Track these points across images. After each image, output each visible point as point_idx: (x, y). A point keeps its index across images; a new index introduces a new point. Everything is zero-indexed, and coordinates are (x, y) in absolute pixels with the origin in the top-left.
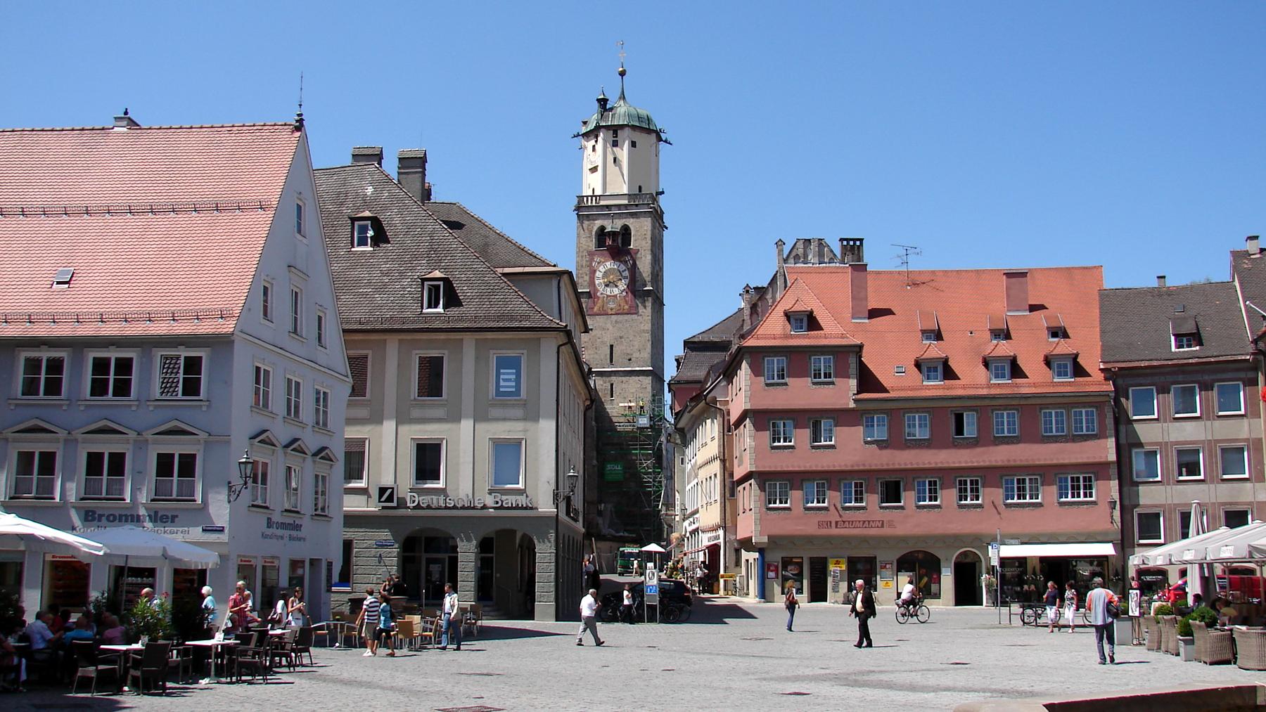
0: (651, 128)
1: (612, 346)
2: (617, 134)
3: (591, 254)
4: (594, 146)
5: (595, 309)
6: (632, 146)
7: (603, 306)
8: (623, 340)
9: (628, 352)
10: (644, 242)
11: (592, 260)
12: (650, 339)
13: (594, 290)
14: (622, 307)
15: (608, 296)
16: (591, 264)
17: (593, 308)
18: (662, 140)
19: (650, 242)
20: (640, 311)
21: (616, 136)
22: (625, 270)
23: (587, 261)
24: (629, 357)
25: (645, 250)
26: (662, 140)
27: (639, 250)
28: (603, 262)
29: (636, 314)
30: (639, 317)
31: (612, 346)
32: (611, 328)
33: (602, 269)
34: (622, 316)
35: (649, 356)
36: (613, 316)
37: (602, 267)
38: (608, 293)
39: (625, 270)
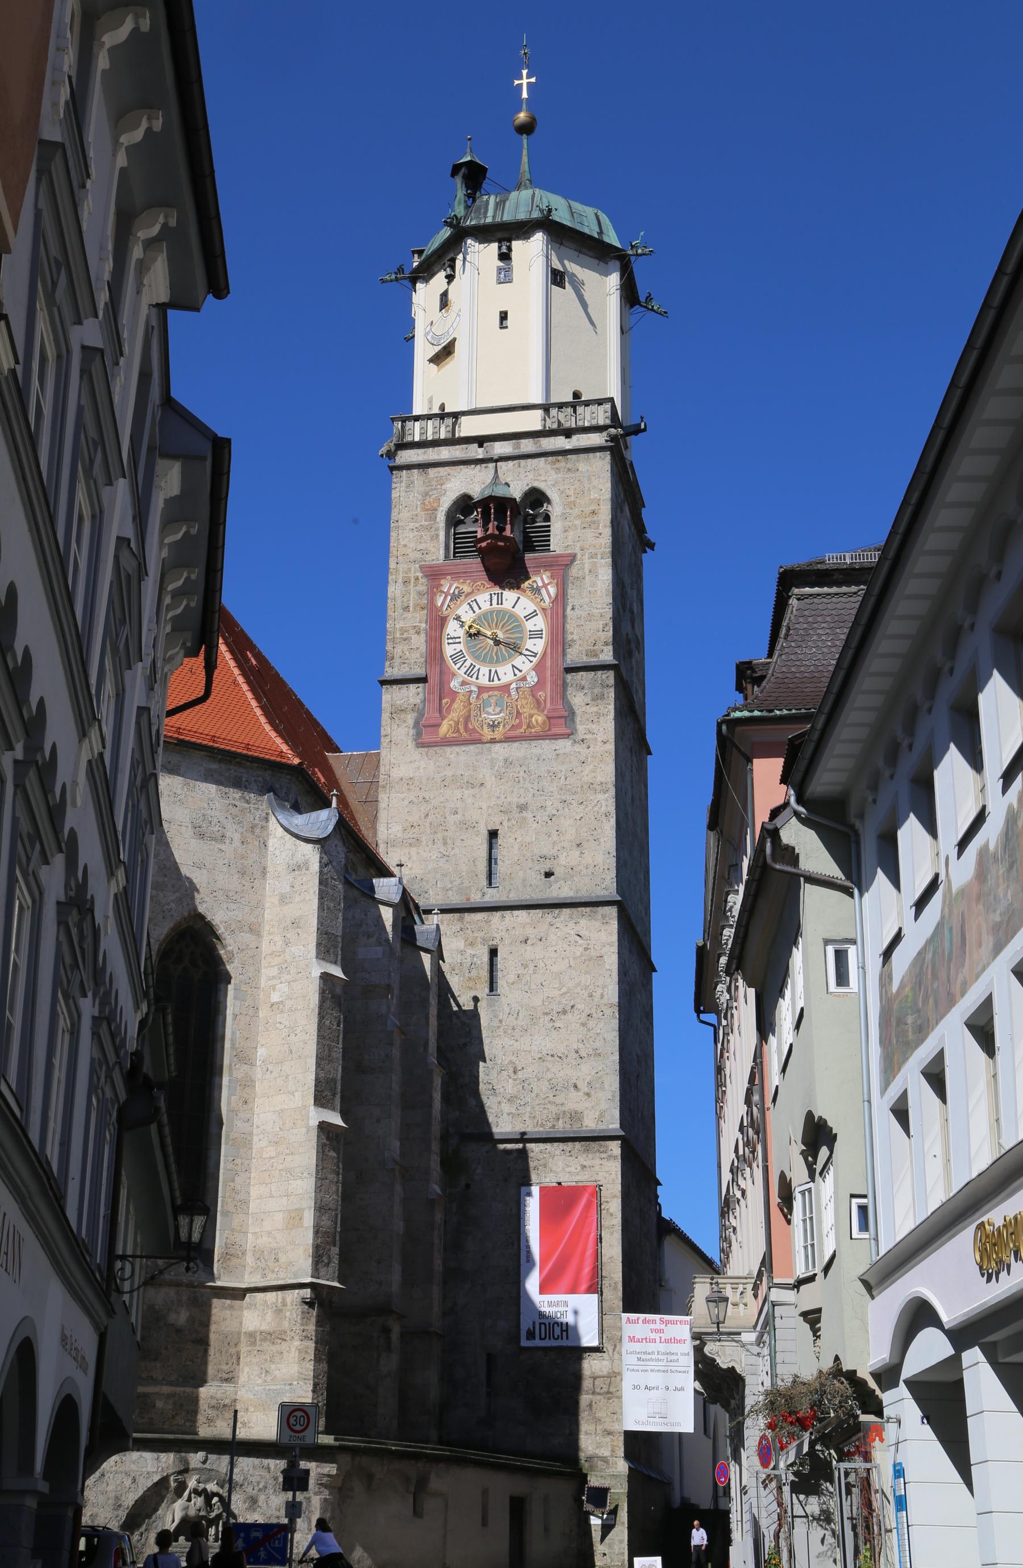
0: (606, 239)
1: (493, 835)
2: (510, 249)
3: (434, 575)
4: (444, 295)
5: (444, 728)
7: (467, 719)
8: (528, 815)
9: (545, 852)
10: (590, 534)
11: (434, 588)
13: (441, 673)
15: (482, 689)
17: (438, 725)
18: (639, 303)
19: (607, 532)
20: (581, 729)
21: (505, 257)
22: (534, 614)
23: (419, 593)
24: (546, 867)
25: (593, 556)
28: (468, 595)
29: (567, 736)
30: (579, 748)
31: (493, 835)
32: (490, 781)
34: (525, 744)
37: (465, 607)
38: (484, 681)
39: (534, 614)
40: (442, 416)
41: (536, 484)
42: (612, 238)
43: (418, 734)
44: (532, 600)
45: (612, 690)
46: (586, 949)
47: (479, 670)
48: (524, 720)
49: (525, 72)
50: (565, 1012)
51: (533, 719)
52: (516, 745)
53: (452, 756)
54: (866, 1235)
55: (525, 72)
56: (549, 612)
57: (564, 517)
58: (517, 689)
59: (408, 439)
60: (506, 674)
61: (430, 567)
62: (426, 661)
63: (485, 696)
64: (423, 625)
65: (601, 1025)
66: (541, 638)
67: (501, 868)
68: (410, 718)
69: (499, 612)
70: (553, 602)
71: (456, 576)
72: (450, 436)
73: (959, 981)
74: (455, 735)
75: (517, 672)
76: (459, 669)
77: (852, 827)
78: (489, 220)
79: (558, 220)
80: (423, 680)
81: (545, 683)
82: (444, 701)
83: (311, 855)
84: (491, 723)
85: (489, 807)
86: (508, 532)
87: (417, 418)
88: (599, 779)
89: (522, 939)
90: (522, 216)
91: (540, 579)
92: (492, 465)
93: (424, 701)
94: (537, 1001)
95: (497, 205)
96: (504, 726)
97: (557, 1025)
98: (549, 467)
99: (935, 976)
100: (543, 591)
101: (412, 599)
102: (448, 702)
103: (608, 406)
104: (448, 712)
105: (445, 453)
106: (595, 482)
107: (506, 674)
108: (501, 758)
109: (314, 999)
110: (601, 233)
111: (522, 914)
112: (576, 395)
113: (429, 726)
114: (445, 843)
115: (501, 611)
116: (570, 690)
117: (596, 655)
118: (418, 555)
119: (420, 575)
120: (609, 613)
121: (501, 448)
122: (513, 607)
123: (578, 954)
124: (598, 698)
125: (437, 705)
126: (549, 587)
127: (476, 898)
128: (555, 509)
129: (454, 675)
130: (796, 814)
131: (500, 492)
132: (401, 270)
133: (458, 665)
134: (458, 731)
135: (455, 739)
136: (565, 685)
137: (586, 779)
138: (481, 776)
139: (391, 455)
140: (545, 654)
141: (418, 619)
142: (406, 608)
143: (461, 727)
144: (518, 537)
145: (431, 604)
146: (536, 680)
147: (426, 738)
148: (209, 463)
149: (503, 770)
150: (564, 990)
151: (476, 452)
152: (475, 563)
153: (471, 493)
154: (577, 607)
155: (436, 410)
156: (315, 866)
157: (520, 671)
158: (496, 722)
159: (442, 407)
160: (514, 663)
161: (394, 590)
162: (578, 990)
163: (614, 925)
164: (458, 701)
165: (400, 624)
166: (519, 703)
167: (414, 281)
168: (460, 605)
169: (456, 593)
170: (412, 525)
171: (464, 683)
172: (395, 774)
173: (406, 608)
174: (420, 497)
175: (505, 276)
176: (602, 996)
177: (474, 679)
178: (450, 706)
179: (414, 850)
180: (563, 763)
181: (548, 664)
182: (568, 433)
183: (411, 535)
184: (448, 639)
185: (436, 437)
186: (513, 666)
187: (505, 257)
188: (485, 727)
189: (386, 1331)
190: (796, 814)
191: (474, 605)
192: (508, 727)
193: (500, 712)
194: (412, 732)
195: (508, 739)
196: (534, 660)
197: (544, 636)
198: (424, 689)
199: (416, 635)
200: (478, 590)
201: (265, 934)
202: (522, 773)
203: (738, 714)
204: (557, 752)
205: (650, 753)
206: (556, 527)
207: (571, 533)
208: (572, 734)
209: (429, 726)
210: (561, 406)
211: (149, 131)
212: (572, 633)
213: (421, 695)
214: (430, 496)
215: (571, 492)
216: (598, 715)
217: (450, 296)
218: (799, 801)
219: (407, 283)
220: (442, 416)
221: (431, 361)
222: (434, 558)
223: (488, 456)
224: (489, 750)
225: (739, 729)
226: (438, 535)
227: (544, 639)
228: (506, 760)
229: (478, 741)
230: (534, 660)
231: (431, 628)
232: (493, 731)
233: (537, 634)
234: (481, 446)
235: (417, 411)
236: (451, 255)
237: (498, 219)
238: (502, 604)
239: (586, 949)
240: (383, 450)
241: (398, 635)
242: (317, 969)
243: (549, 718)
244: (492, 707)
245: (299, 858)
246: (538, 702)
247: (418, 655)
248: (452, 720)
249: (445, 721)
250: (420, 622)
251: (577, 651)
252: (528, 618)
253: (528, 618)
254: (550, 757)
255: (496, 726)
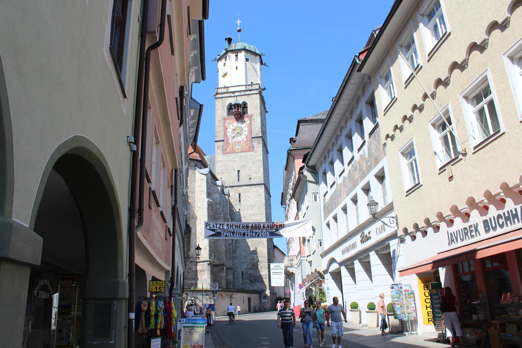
0: (256, 52)
1: (239, 171)
2: (237, 54)
3: (224, 119)
5: (228, 150)
6: (247, 61)
7: (233, 148)
10: (256, 110)
11: (225, 122)
12: (262, 165)
13: (227, 139)
14: (244, 148)
15: (235, 142)
16: (224, 125)
17: (227, 150)
18: (263, 64)
19: (259, 110)
20: (255, 149)
21: (236, 56)
23: (222, 123)
26: (263, 64)
27: (253, 115)
28: (232, 123)
30: (255, 153)
31: (239, 171)
33: (231, 127)
34: (244, 153)
35: (263, 176)
36: (239, 154)
37: (231, 126)
38: (236, 140)
40: (225, 88)
41: (245, 101)
42: (258, 52)
43: (223, 151)
45: (261, 141)
46: (258, 193)
49: (239, 20)
50: (254, 206)
52: (243, 153)
54: (321, 247)
55: (239, 20)
57: (250, 107)
59: (218, 92)
60: (240, 139)
61: (224, 118)
63: (236, 143)
64: (223, 129)
65: (262, 208)
67: (240, 178)
68: (221, 148)
69: (238, 126)
71: (229, 119)
72: (227, 91)
73: (340, 200)
77: (317, 171)
78: (233, 49)
79: (247, 48)
80: (223, 141)
81: (248, 141)
83: (205, 177)
85: (237, 166)
86: (239, 111)
87: (220, 88)
88: (259, 159)
89: (245, 192)
90: (240, 48)
91: (246, 119)
92: (235, 97)
93: (224, 145)
94: (249, 204)
95: (234, 46)
97: (253, 208)
98: (247, 97)
99: (335, 200)
100: (247, 122)
101: (220, 124)
103: (259, 85)
104: (229, 147)
105: (226, 95)
106: (256, 100)
107: (240, 139)
108: (240, 156)
109: (207, 206)
110: (255, 51)
111: (245, 187)
112: (252, 83)
114: (229, 173)
116: (253, 142)
117: (258, 135)
118: (221, 115)
120: (260, 126)
121: (237, 94)
123: (257, 194)
124: (259, 143)
125: (226, 146)
127: (236, 184)
128: (249, 106)
129: (229, 139)
130: (306, 169)
131: (238, 103)
132: (216, 59)
136: (252, 141)
137: (257, 159)
139: (215, 96)
140: (247, 135)
141: (222, 128)
142: (219, 126)
143: (231, 150)
144: (241, 111)
145: (224, 126)
146: (246, 140)
147: (224, 152)
148: (199, 109)
150: (254, 201)
151: (233, 95)
152: (233, 117)
153: (231, 103)
155: (224, 86)
156: (205, 180)
159: (225, 86)
160: (242, 137)
161: (217, 122)
162: (257, 201)
163: (264, 188)
165: (218, 129)
167: (218, 61)
171: (231, 141)
172: (219, 159)
173: (219, 126)
175: (237, 59)
176: (262, 202)
177: (233, 140)
179: (223, 175)
180: (252, 156)
181: (248, 136)
182: (251, 91)
185: (224, 92)
187: (236, 56)
188: (236, 150)
189: (223, 268)
190: (306, 169)
191: (233, 125)
194: (221, 151)
195: (241, 152)
201: (196, 193)
203: (291, 149)
205: (268, 153)
206: (249, 109)
207: (252, 110)
210: (249, 85)
211: (194, 54)
215: (251, 102)
216: (259, 147)
217: (226, 64)
218: (307, 167)
219: (217, 61)
220: (225, 88)
221: (222, 76)
223: (235, 95)
224: (237, 154)
225: (292, 151)
226: (225, 111)
228: (241, 156)
229: (235, 153)
230: (246, 136)
233: (246, 131)
234: (233, 93)
235: (219, 87)
236: (226, 56)
237: (235, 49)
239: (258, 193)
240: (213, 95)
241: (218, 132)
242: (207, 200)
243: (249, 147)
245: (202, 178)
246: (247, 144)
252: (244, 127)
253: (244, 127)
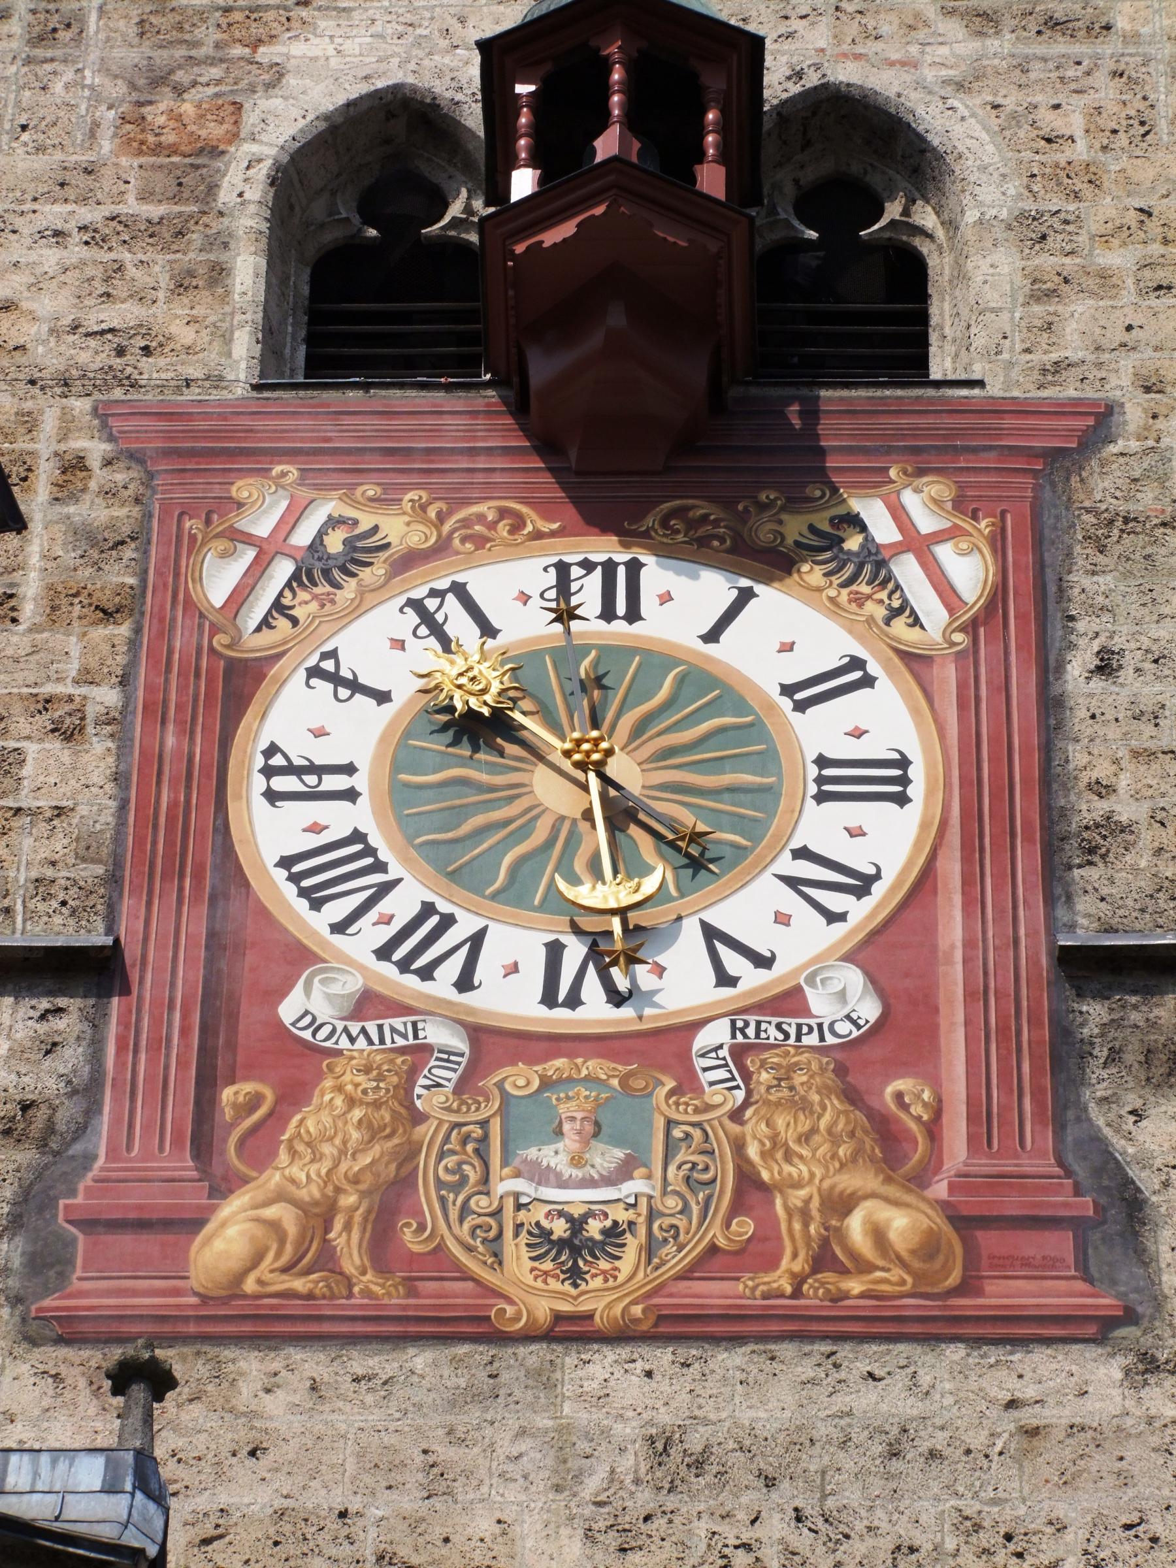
28: (410, 560)
44: (834, 608)
47: (477, 941)
48: (789, 1229)
51: (855, 1225)
53: (274, 1405)
56: (947, 676)
58: (739, 1053)
62: (113, 879)
64: (107, 696)
66: (902, 800)
70: (971, 627)
74: (300, 1285)
75: (733, 962)
76: (339, 928)
82: (227, 1094)
84: (560, 1228)
96: (650, 1249)
100: (907, 570)
102: (254, 1102)
108: (625, 1430)
113: (116, 1225)
115: (633, 651)
119: (96, 449)
122: (712, 636)
126: (945, 552)
133: (337, 910)
134: (327, 1260)
135: (295, 1307)
138: (485, 1526)
146: (869, 1011)
149: (644, 1499)
154: (1130, 661)
157: (763, 962)
158: (594, 1228)
164: (326, 1093)
166: (755, 1131)
168: (356, 610)
169: (335, 543)
170: (53, 214)
174: (118, 89)
178: (277, 1118)
180: (1067, 1482)
183: (50, 257)
184: (269, 772)
186: (711, 934)
188: (517, 1253)
192: (674, 1260)
193: (624, 1172)
196: (859, 910)
197: (916, 790)
198: (96, 1023)
199: (55, 745)
200: (480, 542)
202: (776, 1527)
204: (1028, 1416)
208: (1130, 1317)
209: (116, 1225)
212: (1102, 789)
213: (72, 1057)
214: (179, 91)
222: (194, 371)
226: (219, 273)
227: (914, 812)
230: (859, 910)
231: (156, 712)
232: (575, 1275)
238: (633, 615)
244: (570, 1142)
247: (59, 845)
248: (280, 1197)
249: (234, 1205)
250: (87, 677)
251: (1145, 884)
254: (977, 1440)
255: (594, 1248)
